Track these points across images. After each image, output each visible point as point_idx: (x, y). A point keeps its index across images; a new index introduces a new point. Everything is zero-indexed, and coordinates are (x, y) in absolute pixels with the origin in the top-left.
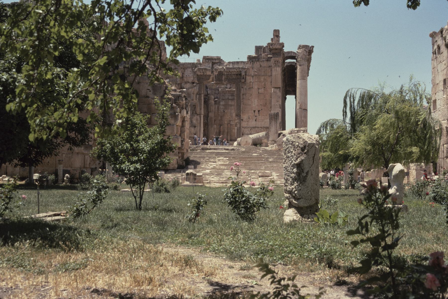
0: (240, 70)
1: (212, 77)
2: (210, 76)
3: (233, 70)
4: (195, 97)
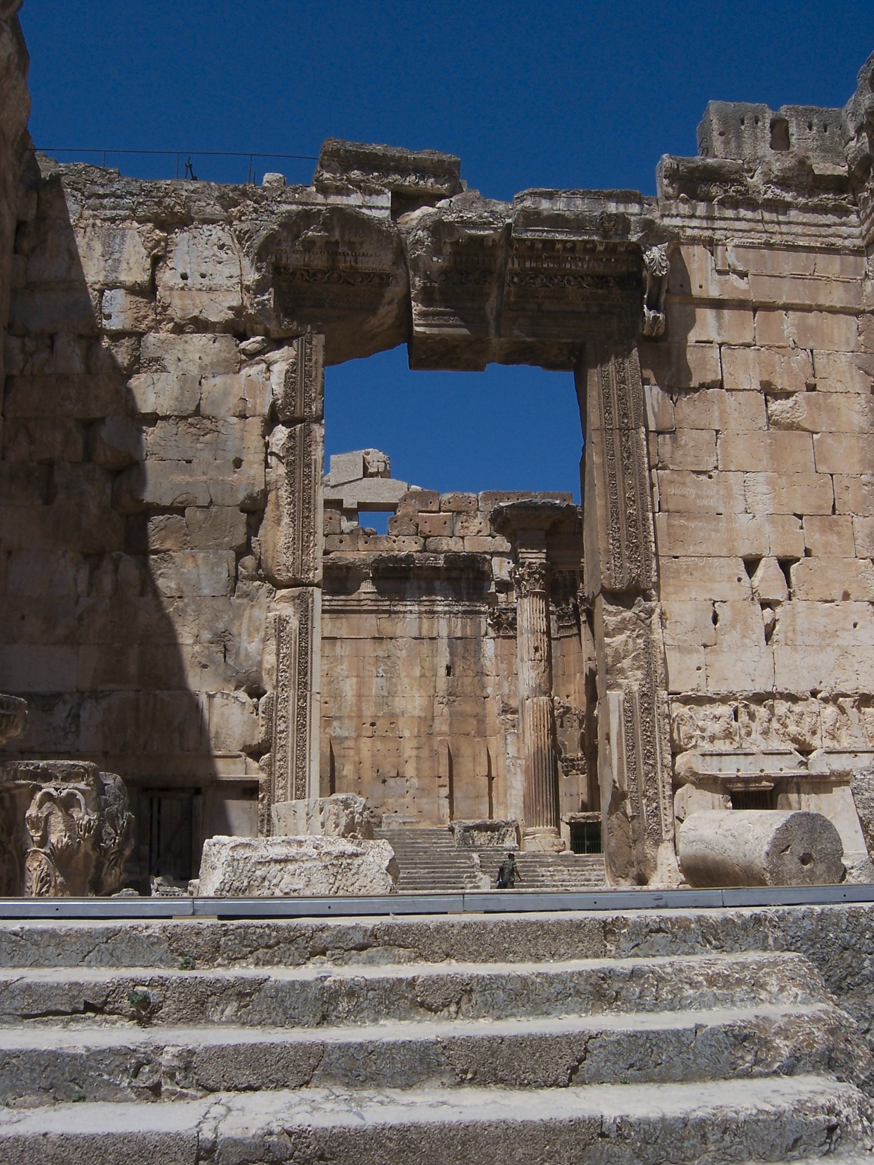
4: (254, 440)
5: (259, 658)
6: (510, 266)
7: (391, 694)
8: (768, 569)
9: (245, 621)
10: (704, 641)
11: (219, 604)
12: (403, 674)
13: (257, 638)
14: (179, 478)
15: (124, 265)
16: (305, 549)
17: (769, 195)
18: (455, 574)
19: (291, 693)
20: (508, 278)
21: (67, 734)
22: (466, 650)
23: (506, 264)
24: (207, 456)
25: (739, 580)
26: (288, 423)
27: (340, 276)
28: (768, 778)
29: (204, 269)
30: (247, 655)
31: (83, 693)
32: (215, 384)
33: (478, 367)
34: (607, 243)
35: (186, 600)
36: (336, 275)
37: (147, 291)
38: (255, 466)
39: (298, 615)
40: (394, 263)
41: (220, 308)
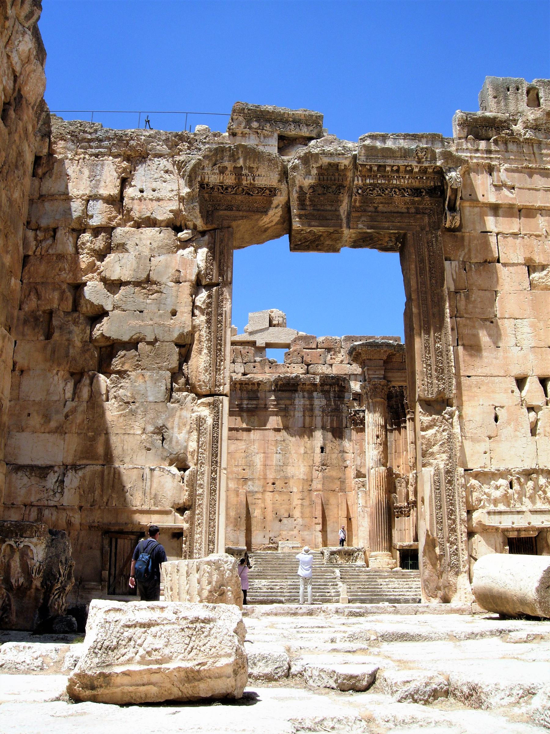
0: (439, 163)
1: (280, 199)
2: (273, 192)
3: (401, 163)
5: (186, 444)
6: (356, 182)
7: (285, 464)
8: (532, 385)
9: (177, 419)
10: (489, 433)
11: (160, 407)
12: (293, 452)
13: (185, 430)
14: (134, 322)
15: (102, 184)
16: (217, 370)
17: (527, 136)
18: (326, 388)
19: (206, 468)
20: (355, 190)
21: (55, 494)
23: (353, 181)
24: (154, 308)
25: (512, 392)
26: (208, 287)
27: (243, 189)
28: (533, 529)
29: (154, 185)
30: (177, 442)
31: (67, 466)
32: (160, 260)
33: (336, 250)
34: (421, 167)
35: (137, 404)
36: (240, 189)
37: (116, 202)
38: (185, 315)
39: (212, 415)
40: (279, 181)
41: (165, 211)
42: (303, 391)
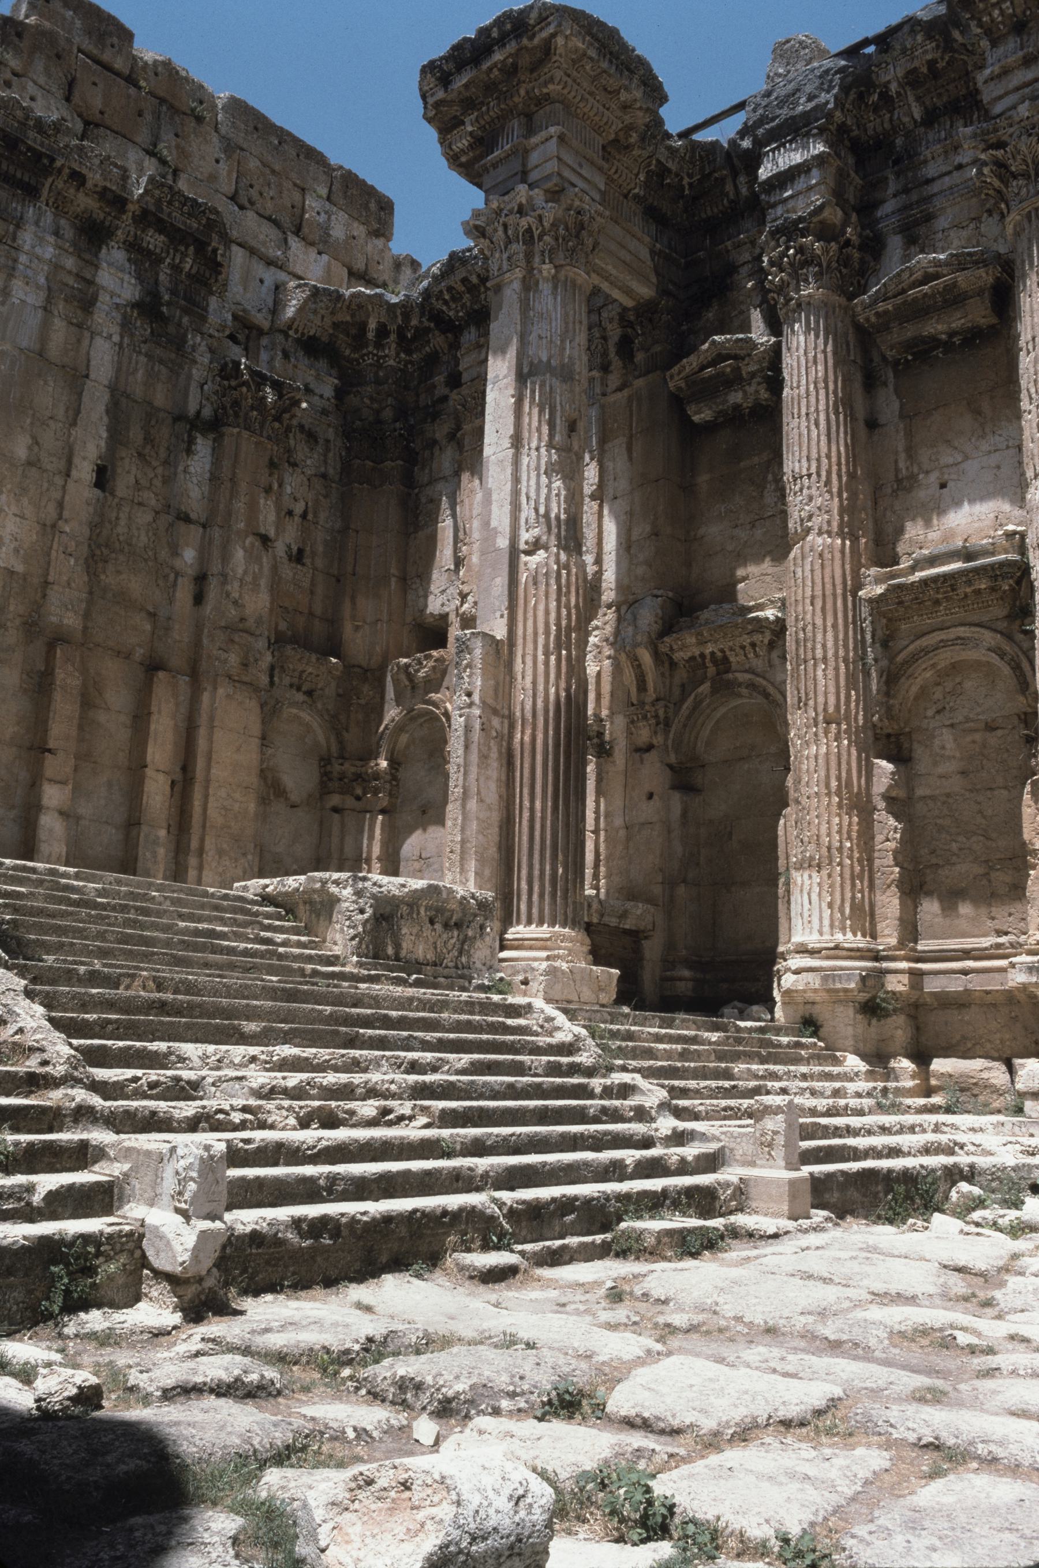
22: (148, 440)
42: (60, 206)
